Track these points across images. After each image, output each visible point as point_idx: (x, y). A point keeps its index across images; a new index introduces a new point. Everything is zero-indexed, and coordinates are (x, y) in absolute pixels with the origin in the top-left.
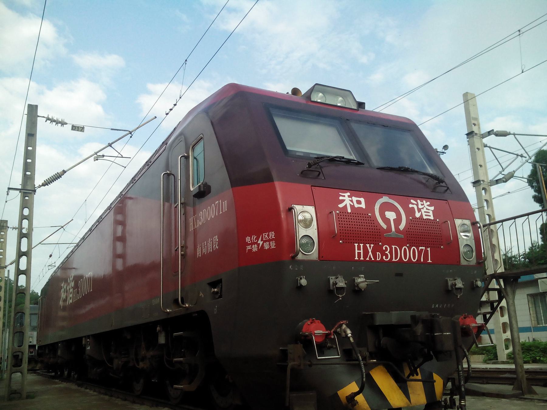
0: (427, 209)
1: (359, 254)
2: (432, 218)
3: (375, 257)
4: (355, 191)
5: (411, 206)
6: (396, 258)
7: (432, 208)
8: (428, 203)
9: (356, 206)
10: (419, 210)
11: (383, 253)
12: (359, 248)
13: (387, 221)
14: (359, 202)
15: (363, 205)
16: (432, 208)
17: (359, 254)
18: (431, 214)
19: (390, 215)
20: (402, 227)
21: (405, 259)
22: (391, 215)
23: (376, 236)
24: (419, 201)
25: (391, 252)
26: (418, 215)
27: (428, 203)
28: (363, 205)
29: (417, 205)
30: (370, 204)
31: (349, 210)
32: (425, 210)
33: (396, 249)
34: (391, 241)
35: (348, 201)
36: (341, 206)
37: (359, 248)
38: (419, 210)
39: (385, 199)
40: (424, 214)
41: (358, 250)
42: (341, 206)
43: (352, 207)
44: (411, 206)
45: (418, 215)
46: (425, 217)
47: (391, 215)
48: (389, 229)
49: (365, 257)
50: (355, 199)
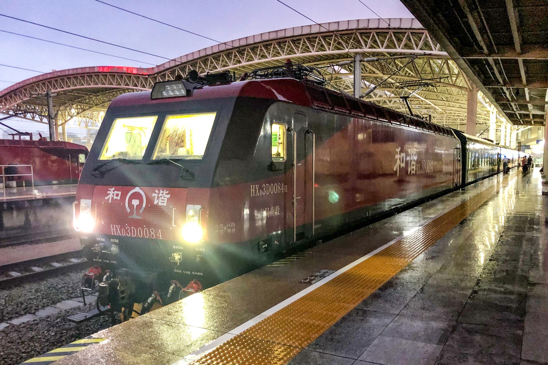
0: (164, 197)
7: (169, 196)
8: (168, 192)
9: (115, 197)
10: (158, 198)
12: (113, 227)
16: (169, 196)
18: (166, 199)
24: (161, 192)
27: (168, 192)
29: (159, 194)
31: (110, 202)
32: (162, 198)
36: (106, 198)
38: (158, 198)
40: (160, 201)
43: (113, 198)
44: (154, 195)
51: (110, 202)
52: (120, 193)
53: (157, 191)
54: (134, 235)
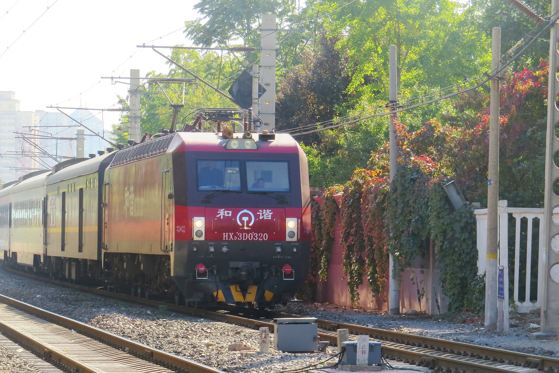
1: (225, 238)
2: (270, 218)
3: (234, 238)
5: (258, 213)
6: (245, 238)
7: (272, 213)
9: (226, 215)
10: (263, 215)
11: (238, 237)
12: (226, 235)
13: (242, 222)
14: (228, 213)
15: (230, 215)
16: (272, 213)
17: (225, 238)
18: (270, 216)
19: (245, 218)
20: (250, 225)
21: (251, 238)
23: (236, 229)
26: (261, 218)
28: (230, 215)
29: (262, 213)
30: (234, 215)
31: (222, 218)
32: (267, 214)
33: (245, 235)
35: (222, 213)
36: (217, 216)
37: (226, 235)
38: (263, 215)
39: (245, 211)
40: (265, 217)
41: (225, 236)
42: (217, 216)
44: (258, 213)
45: (261, 218)
46: (265, 218)
47: (245, 219)
48: (243, 226)
49: (229, 238)
50: (226, 212)
51: (222, 218)
52: (230, 212)
53: (260, 211)
54: (245, 238)
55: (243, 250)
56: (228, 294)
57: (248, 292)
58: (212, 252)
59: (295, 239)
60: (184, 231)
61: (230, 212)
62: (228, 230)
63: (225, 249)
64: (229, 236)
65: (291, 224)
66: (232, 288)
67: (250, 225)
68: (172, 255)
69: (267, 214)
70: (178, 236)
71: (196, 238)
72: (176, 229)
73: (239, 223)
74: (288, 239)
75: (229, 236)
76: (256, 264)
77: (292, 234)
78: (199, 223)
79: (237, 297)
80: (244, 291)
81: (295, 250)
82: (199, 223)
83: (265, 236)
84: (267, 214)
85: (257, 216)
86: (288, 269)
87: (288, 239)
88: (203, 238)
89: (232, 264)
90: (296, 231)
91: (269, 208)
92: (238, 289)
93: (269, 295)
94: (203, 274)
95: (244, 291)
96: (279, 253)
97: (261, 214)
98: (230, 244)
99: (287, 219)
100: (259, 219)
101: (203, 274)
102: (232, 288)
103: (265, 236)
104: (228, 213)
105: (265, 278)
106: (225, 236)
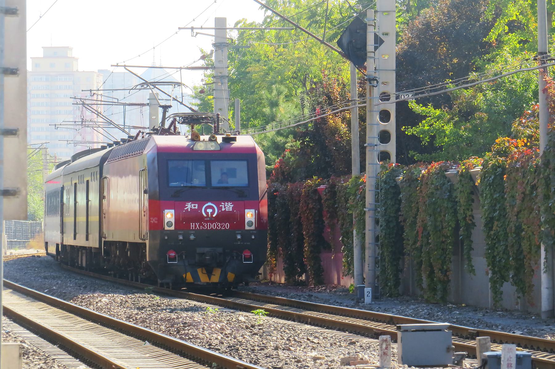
4: (193, 202)
7: (232, 206)
10: (225, 207)
11: (203, 226)
13: (207, 213)
14: (195, 206)
15: (196, 208)
16: (232, 206)
19: (210, 209)
20: (214, 216)
22: (209, 211)
25: (207, 226)
26: (223, 210)
28: (196, 208)
30: (200, 208)
34: (207, 222)
35: (189, 206)
38: (225, 207)
39: (210, 204)
41: (192, 226)
45: (223, 210)
47: (209, 211)
50: (193, 205)
52: (197, 205)
55: (208, 238)
56: (195, 276)
57: (213, 273)
58: (181, 240)
59: (253, 228)
60: (156, 222)
61: (197, 205)
62: (195, 221)
63: (192, 237)
64: (196, 226)
65: (250, 215)
66: (199, 271)
67: (214, 216)
68: (147, 242)
69: (228, 207)
70: (152, 227)
71: (167, 228)
72: (150, 220)
73: (204, 214)
74: (247, 228)
75: (196, 226)
76: (220, 250)
77: (250, 224)
78: (169, 215)
79: (204, 278)
80: (209, 273)
81: (253, 237)
82: (169, 215)
83: (227, 226)
84: (228, 207)
85: (220, 208)
86: (247, 254)
87: (247, 228)
88: (173, 228)
89: (199, 250)
90: (253, 221)
91: (230, 201)
92: (205, 272)
93: (231, 276)
94: (174, 259)
95: (209, 273)
96: (239, 239)
97: (223, 206)
98: (197, 232)
99: (246, 211)
100: (222, 211)
101: (174, 259)
102: (199, 271)
103: (227, 226)
104: (195, 206)
105: (227, 261)
106: (192, 226)
